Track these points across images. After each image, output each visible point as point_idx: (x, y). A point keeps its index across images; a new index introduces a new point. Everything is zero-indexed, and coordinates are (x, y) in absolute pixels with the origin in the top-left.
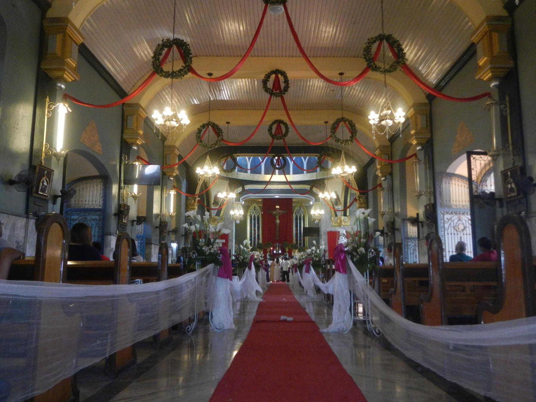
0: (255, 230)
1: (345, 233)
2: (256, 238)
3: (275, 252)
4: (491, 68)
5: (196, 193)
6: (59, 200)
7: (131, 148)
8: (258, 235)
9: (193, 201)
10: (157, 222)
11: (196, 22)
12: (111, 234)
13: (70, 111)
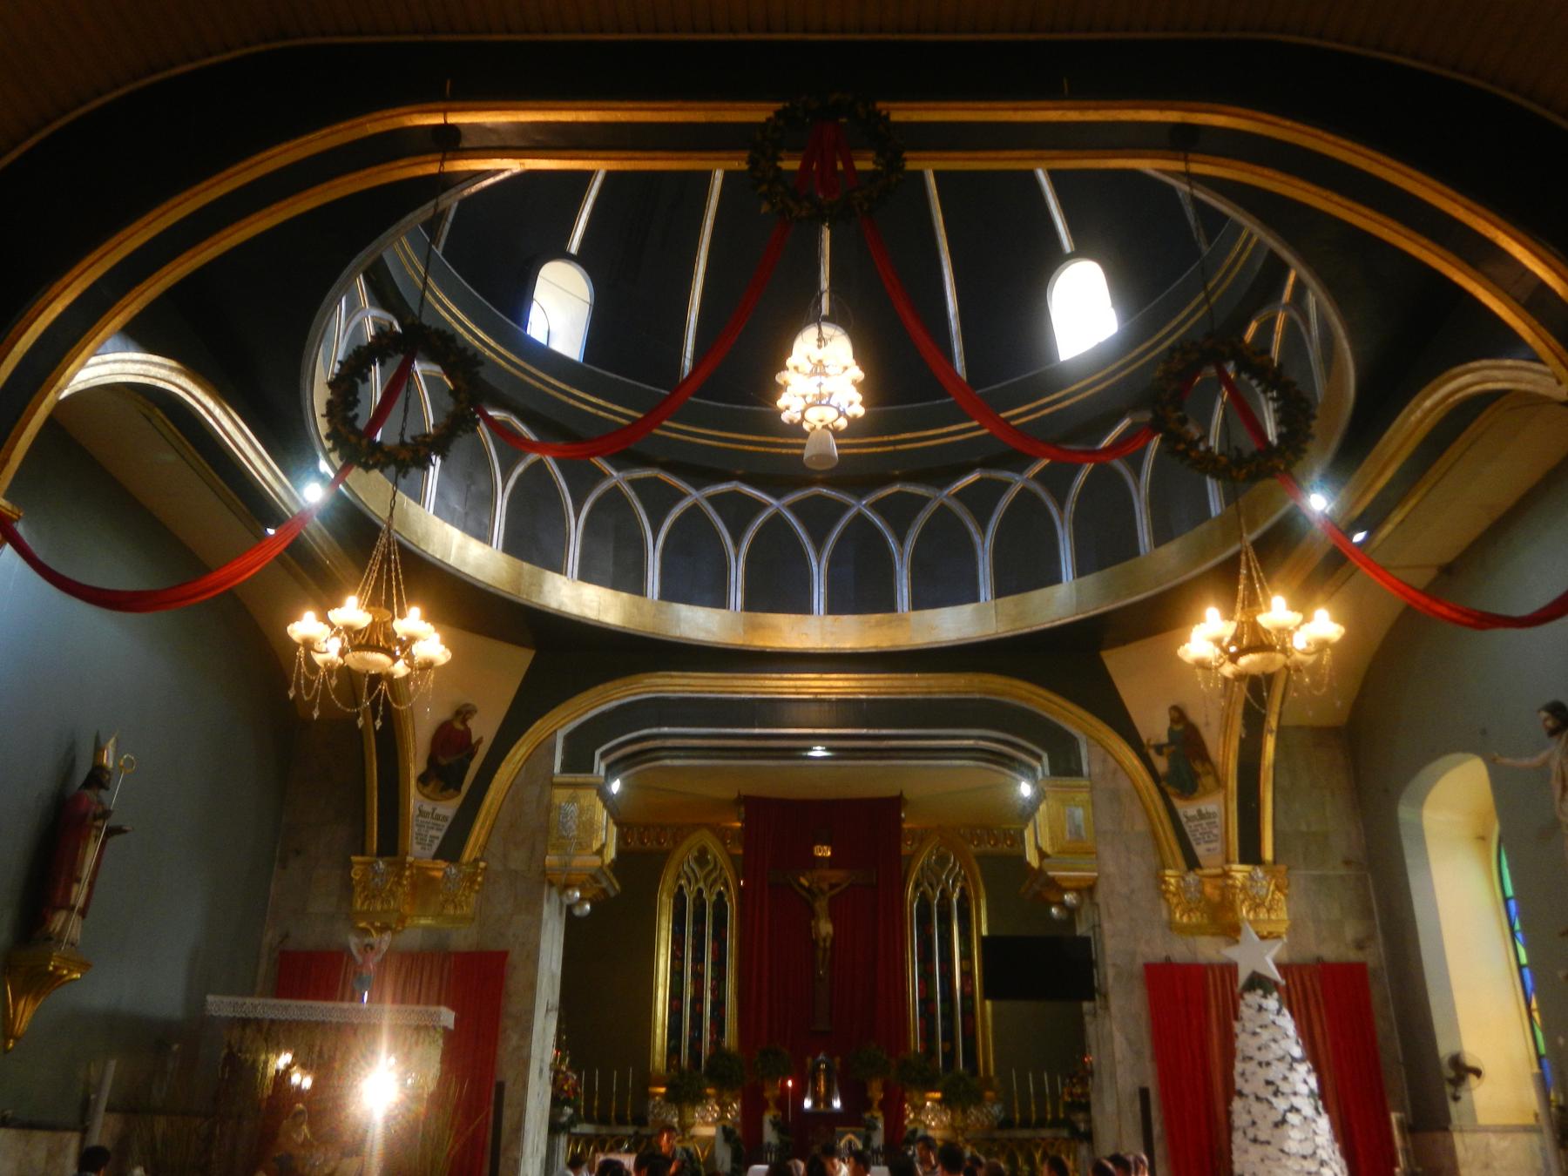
0: (698, 977)
1: (1275, 975)
2: (707, 1024)
3: (808, 1104)
8: (718, 1005)
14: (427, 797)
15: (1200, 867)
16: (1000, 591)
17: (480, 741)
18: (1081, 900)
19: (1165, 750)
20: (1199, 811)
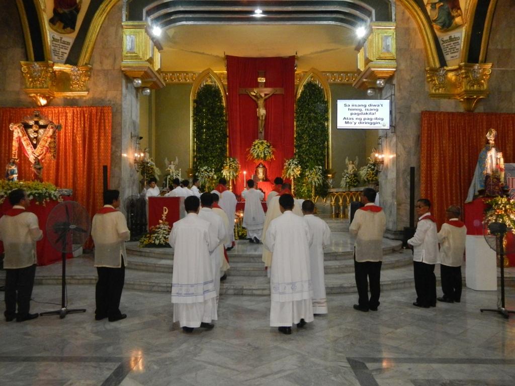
14: (56, 30)
15: (446, 66)
17: (81, 2)
18: (386, 83)
19: (437, 6)
20: (450, 37)
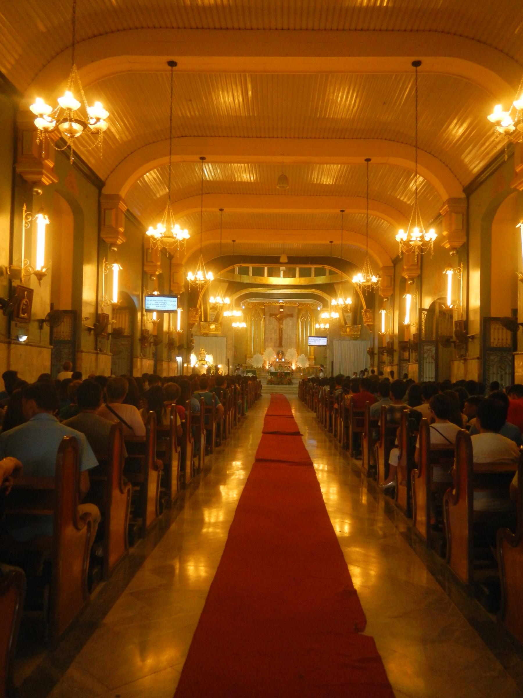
4: (449, 242)
5: (191, 297)
6: (110, 336)
7: (150, 278)
9: (195, 313)
10: (165, 340)
11: (213, 174)
12: (137, 357)
13: (121, 268)
16: (315, 276)
